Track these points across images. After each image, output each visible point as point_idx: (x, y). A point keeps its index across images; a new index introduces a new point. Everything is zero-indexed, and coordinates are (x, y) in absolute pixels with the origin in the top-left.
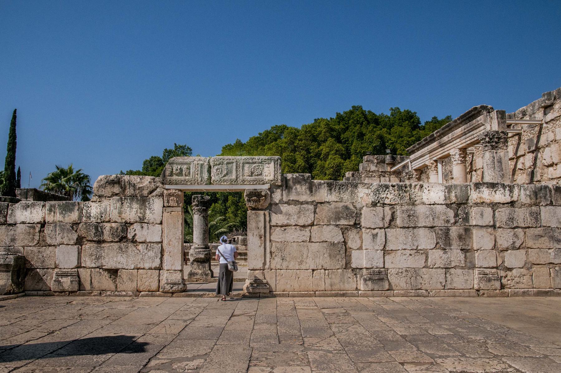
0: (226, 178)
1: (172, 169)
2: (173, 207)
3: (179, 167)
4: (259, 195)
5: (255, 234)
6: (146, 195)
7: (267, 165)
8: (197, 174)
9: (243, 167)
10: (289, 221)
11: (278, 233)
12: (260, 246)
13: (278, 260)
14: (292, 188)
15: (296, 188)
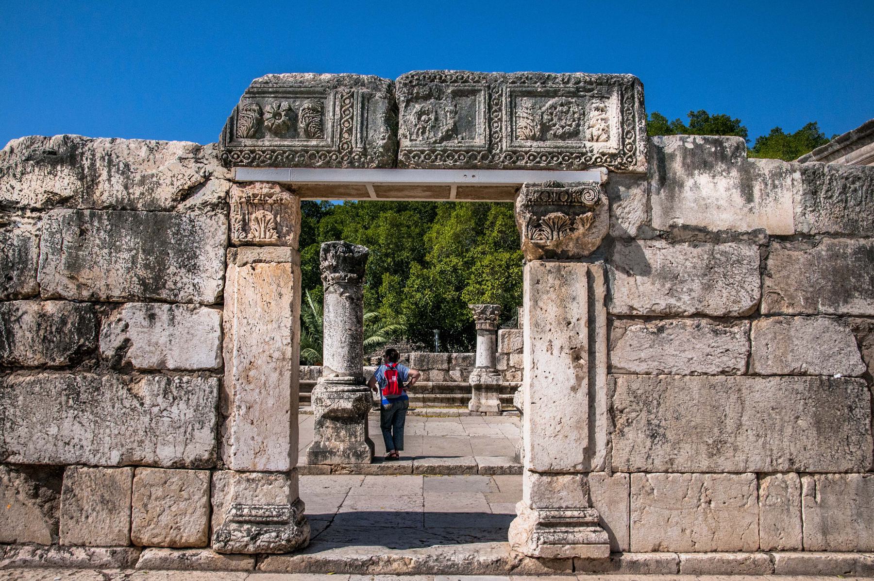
0: (453, 144)
1: (261, 114)
2: (261, 245)
3: (285, 105)
4: (571, 205)
5: (557, 344)
6: (169, 203)
7: (596, 103)
8: (350, 131)
9: (513, 106)
10: (673, 301)
11: (635, 343)
12: (574, 389)
13: (636, 436)
14: (681, 186)
15: (696, 186)
